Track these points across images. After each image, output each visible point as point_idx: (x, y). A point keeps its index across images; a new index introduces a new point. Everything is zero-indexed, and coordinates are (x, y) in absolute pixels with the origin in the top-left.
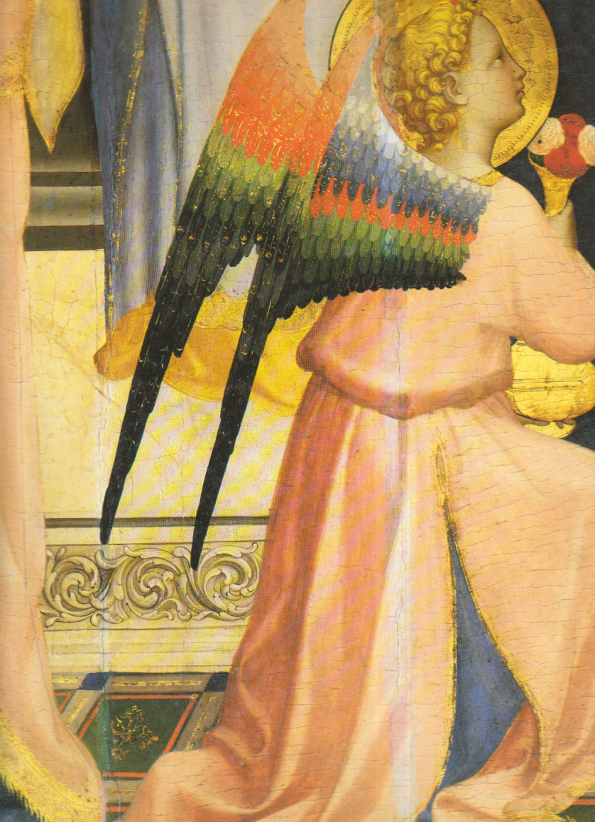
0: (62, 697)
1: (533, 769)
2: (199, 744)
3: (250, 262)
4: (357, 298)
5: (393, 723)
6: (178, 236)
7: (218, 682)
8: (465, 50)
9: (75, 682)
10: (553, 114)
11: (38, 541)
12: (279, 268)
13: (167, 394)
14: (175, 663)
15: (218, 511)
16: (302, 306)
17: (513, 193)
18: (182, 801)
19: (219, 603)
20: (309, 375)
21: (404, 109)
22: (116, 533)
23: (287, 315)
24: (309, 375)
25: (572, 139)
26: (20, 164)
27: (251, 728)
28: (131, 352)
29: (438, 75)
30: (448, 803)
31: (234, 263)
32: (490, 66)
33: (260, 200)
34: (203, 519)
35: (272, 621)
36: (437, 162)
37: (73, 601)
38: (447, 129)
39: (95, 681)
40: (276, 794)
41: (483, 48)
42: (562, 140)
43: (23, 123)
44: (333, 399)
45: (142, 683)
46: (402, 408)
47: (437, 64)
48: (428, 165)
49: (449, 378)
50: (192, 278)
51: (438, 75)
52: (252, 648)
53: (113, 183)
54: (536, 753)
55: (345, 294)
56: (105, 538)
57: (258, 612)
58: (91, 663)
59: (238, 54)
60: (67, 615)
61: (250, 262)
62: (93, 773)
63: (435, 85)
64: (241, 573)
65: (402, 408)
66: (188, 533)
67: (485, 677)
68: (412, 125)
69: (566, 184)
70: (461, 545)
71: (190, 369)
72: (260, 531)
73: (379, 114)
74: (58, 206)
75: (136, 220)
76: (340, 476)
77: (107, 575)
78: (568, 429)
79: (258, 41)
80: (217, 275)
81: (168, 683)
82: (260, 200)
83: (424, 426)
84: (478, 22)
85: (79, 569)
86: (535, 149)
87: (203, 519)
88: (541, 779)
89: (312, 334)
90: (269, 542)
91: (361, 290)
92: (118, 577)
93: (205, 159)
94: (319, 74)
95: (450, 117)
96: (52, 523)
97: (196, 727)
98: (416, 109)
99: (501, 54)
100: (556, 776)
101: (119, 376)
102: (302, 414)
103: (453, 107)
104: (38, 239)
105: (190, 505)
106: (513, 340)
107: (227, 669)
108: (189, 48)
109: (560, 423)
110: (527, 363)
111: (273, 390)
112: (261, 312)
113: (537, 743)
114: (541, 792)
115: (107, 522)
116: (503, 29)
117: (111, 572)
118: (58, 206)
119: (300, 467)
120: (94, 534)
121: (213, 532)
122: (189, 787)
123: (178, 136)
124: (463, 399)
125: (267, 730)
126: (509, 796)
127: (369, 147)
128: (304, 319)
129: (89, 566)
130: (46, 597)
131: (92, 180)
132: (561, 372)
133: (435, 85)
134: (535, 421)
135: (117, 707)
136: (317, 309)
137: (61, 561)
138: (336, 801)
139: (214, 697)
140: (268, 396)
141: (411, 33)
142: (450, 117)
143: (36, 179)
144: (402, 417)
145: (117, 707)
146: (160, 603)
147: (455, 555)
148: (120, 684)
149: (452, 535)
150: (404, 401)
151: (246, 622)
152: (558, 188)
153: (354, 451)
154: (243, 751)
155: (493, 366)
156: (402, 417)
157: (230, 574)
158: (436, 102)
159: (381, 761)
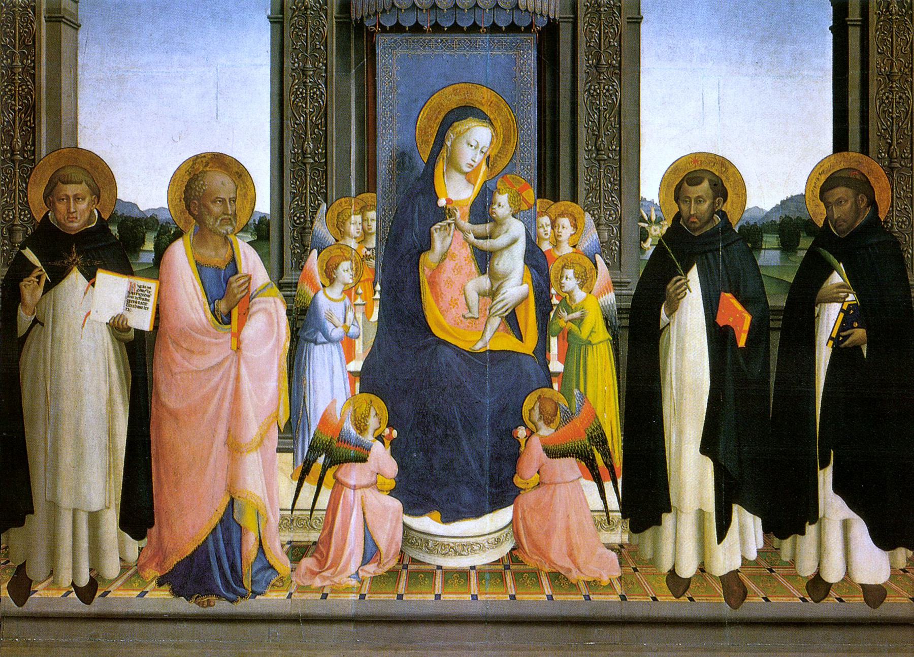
0: (282, 546)
1: (379, 563)
2: (310, 556)
3: (323, 456)
4: (345, 464)
5: (351, 554)
6: (308, 450)
7: (315, 543)
8: (369, 413)
9: (285, 543)
10: (387, 427)
11: (279, 513)
12: (329, 458)
13: (305, 484)
14: (306, 539)
15: (315, 508)
16: (334, 465)
17: (378, 444)
18: (307, 568)
19: (315, 527)
20: (335, 480)
21: (356, 425)
22: (294, 512)
23: (331, 467)
24: (335, 480)
25: (391, 433)
26: (276, 435)
27: (321, 553)
28: (298, 475)
29: (363, 418)
30: (362, 570)
31: (320, 456)
32: (374, 417)
33: (326, 443)
34: (312, 510)
35: (326, 532)
36: (363, 437)
37: (285, 526)
38: (365, 430)
39: (290, 542)
40: (326, 567)
41: (373, 413)
42: (389, 432)
43: (277, 426)
44: (340, 485)
45: (299, 543)
46: (355, 488)
47: (363, 416)
48: (361, 437)
49: (365, 482)
50: (312, 459)
51: (363, 418)
52: (322, 537)
53: (295, 439)
54: (380, 560)
55: (343, 463)
56: (292, 513)
57: (323, 530)
58: (289, 539)
59: (321, 414)
60: (284, 529)
61: (323, 456)
62: (289, 562)
63: (362, 421)
64: (320, 520)
65: (355, 488)
66: (309, 513)
67: (370, 544)
68: (357, 428)
69: (389, 442)
70: (366, 517)
71: (310, 478)
72: (325, 512)
73: (351, 427)
74: (285, 444)
75: (300, 447)
76: (341, 502)
77: (292, 521)
78: (388, 493)
79: (326, 411)
80: (316, 459)
81: (304, 543)
82: (326, 443)
83: (359, 492)
84: (372, 408)
85: (287, 519)
86: (383, 434)
87: (312, 510)
88: (381, 565)
89: (336, 472)
90: (326, 515)
91: (346, 462)
92: (295, 521)
93: (315, 435)
94: (339, 417)
95: (365, 427)
96: (281, 510)
97: (310, 553)
98: (358, 426)
99: (376, 414)
100: (384, 565)
101: (295, 480)
102: (333, 488)
103: (366, 425)
104: (279, 450)
105: (310, 507)
106: (377, 474)
107: (317, 540)
108: (312, 410)
109: (387, 491)
110: (380, 478)
111: (327, 483)
112: (325, 466)
113: (380, 557)
114: (381, 568)
115: (292, 510)
116: (377, 409)
117: (293, 520)
118: (285, 444)
119: (333, 500)
120: (290, 512)
121: (314, 512)
122: (309, 565)
123: (309, 430)
124: (367, 486)
125: (325, 554)
126: (374, 569)
127: (349, 433)
128: (334, 468)
129: (288, 519)
130: (280, 525)
131: (291, 438)
132: (388, 481)
133: (362, 421)
134: (382, 491)
135: (293, 548)
136: (337, 466)
137: (282, 517)
138: (339, 569)
139: (314, 547)
140: (326, 485)
141: (358, 410)
142: (365, 427)
143: (279, 438)
144: (354, 490)
145: (293, 548)
146: (304, 527)
147: (364, 519)
148: (294, 543)
149: (364, 514)
150: (355, 486)
151: (321, 531)
152: (387, 442)
153: (344, 497)
154: (320, 558)
155: (374, 479)
156: (354, 490)
157: (318, 521)
158: (363, 424)
159: (348, 563)
